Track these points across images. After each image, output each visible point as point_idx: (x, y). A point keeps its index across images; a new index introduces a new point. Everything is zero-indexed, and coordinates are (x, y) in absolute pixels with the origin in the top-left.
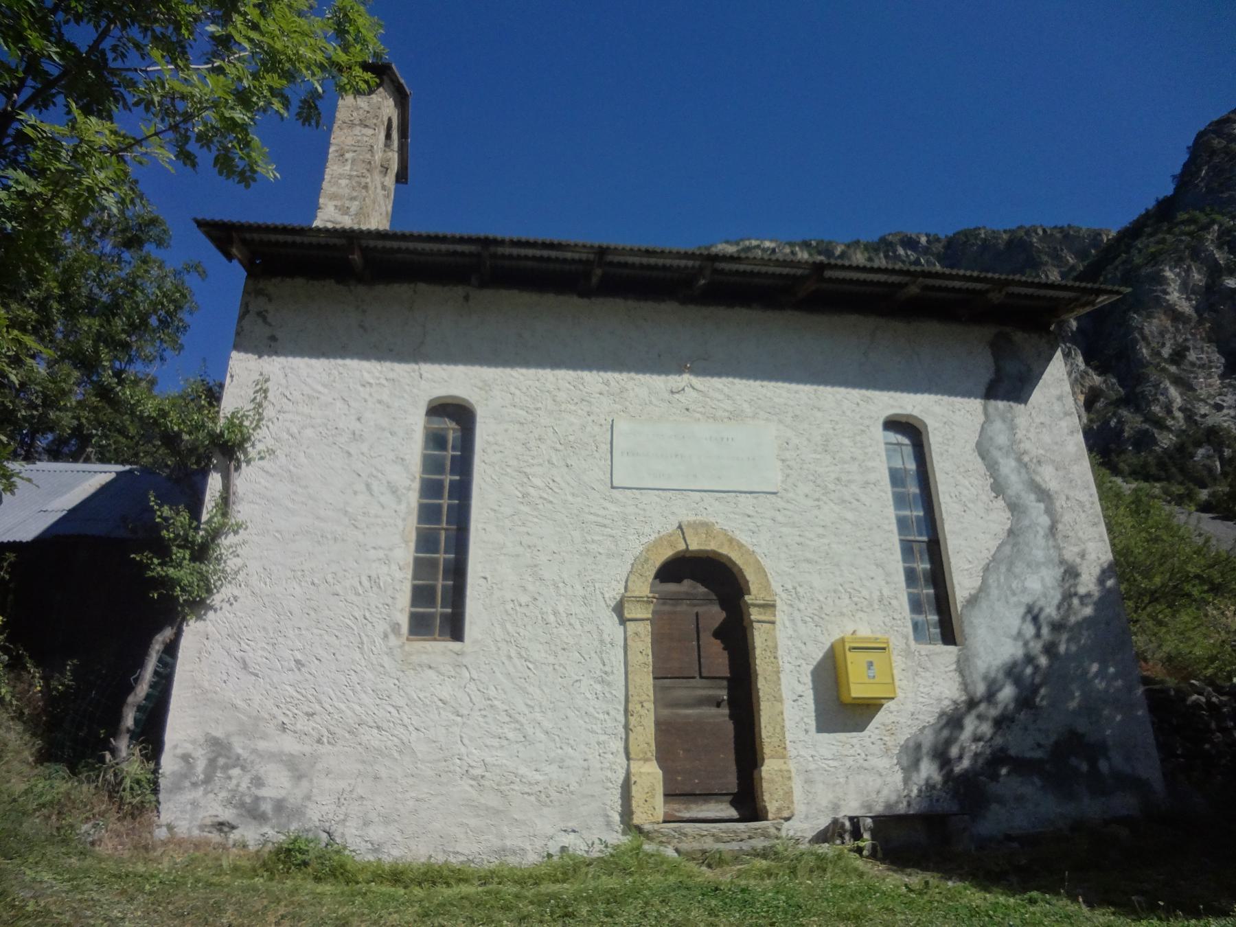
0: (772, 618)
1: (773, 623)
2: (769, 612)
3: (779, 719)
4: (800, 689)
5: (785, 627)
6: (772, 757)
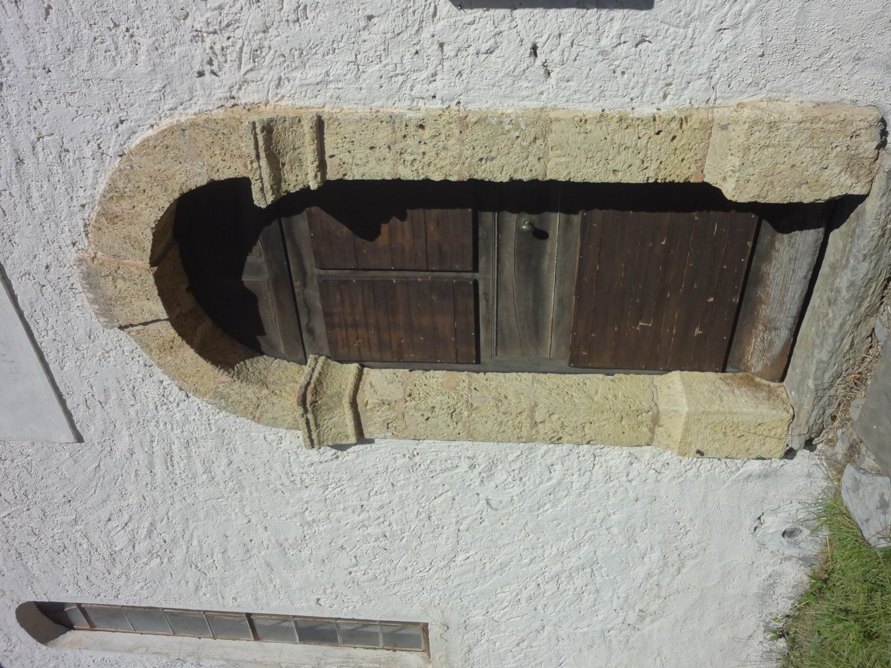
0: (307, 128)
1: (320, 125)
2: (286, 139)
3: (598, 132)
4: (512, 53)
5: (323, 83)
6: (701, 162)
